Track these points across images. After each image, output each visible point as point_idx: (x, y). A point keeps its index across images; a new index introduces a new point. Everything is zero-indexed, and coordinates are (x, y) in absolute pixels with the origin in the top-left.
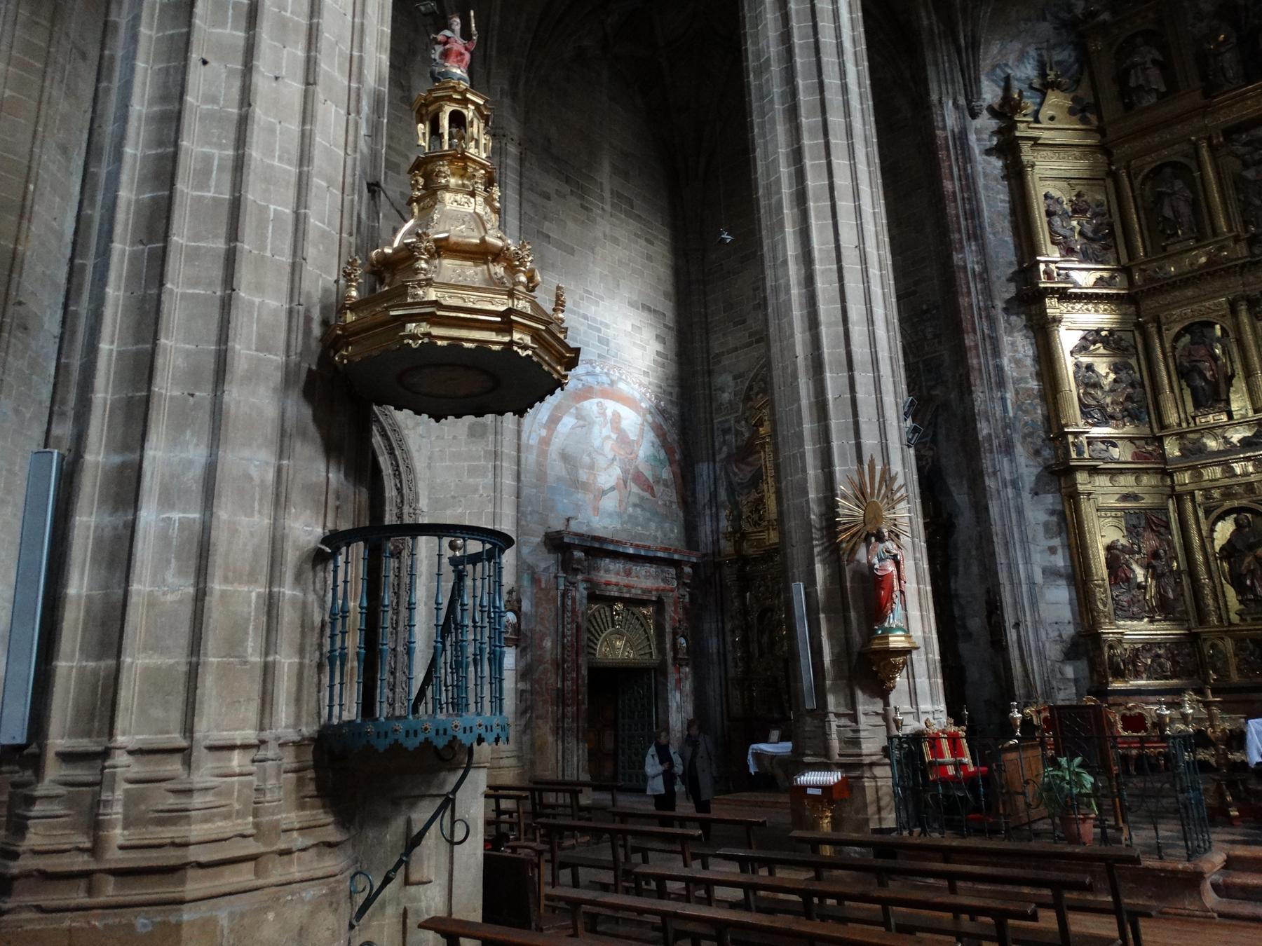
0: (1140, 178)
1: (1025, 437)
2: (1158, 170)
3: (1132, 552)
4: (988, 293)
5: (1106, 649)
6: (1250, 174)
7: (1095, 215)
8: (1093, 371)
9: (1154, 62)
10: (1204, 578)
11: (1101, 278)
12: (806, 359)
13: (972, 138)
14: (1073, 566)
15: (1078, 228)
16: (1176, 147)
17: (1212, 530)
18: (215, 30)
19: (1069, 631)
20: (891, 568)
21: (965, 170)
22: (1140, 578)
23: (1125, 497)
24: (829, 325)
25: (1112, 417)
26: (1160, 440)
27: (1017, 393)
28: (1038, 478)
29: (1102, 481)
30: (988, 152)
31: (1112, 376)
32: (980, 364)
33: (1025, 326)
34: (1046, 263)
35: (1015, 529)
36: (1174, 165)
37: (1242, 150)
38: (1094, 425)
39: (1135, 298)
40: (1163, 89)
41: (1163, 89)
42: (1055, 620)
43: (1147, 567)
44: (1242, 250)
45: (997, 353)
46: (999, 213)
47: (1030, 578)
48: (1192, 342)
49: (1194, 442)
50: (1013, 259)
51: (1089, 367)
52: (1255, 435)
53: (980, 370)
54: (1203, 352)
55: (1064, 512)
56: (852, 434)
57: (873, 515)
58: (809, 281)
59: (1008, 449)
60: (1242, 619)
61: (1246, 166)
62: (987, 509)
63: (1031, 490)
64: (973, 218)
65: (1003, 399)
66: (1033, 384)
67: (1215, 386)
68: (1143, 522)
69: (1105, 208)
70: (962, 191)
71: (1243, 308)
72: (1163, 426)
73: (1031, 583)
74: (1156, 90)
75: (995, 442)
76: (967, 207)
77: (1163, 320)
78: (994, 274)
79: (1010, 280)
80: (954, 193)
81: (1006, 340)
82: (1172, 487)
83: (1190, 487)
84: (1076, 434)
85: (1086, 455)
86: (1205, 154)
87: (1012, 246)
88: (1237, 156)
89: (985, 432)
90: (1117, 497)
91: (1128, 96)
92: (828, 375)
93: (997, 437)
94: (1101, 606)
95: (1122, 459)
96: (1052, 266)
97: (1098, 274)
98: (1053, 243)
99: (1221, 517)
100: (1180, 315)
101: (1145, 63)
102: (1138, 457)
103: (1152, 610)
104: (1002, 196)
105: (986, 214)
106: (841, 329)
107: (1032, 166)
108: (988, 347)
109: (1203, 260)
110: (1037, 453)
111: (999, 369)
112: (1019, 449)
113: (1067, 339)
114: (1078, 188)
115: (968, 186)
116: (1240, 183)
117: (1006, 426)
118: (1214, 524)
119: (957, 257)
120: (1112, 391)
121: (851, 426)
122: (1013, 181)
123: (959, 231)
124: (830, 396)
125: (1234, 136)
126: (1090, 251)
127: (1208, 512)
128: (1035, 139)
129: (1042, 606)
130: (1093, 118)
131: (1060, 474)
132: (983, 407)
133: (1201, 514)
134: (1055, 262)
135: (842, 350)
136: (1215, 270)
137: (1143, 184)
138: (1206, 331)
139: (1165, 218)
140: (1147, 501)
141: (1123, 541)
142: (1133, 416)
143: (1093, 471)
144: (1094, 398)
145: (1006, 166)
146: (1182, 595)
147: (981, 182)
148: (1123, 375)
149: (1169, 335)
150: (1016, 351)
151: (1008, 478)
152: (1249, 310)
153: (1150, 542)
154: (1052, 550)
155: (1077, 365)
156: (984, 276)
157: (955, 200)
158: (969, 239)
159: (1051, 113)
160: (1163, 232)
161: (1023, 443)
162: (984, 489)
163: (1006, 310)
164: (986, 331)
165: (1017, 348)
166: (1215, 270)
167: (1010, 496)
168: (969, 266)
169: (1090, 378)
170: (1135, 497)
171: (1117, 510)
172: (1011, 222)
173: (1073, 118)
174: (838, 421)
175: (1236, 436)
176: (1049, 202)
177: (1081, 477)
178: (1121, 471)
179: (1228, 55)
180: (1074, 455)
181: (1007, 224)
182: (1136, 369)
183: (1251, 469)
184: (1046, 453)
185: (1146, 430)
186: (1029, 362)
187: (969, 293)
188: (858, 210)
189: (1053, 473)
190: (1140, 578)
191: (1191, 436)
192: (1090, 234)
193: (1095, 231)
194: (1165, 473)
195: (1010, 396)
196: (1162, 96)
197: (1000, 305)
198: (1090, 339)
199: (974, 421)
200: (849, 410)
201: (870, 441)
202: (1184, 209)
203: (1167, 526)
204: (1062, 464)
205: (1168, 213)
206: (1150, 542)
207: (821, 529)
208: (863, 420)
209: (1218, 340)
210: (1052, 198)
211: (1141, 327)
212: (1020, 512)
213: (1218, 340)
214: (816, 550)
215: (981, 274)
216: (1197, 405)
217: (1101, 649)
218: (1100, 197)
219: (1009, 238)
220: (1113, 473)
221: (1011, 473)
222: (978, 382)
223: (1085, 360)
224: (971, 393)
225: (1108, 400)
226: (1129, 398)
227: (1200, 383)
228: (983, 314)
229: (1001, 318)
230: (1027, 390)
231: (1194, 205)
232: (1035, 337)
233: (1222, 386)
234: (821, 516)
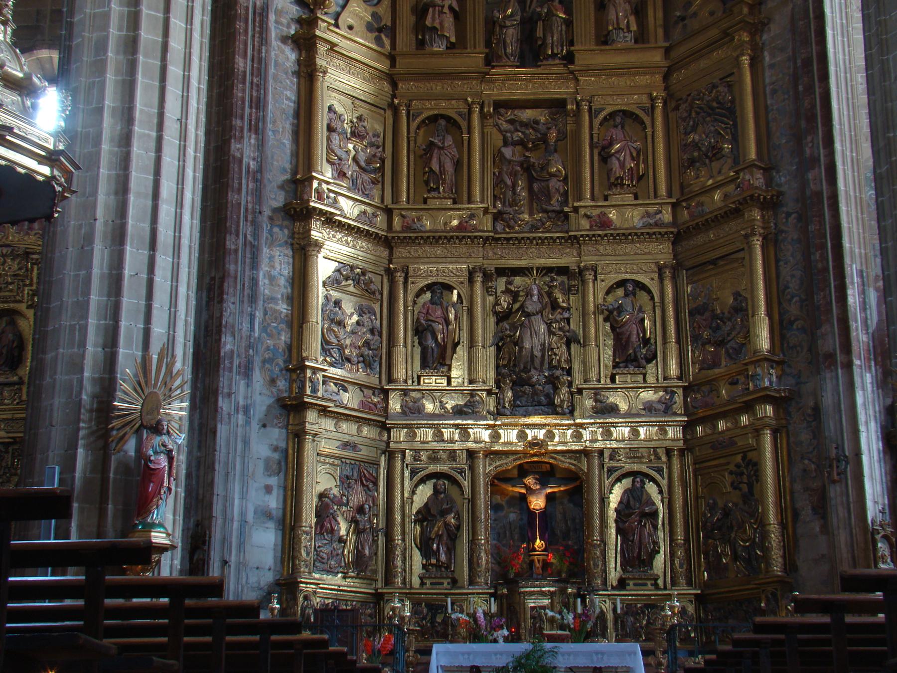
0: (418, 120)
1: (264, 361)
2: (434, 119)
3: (340, 504)
4: (258, 195)
5: (301, 599)
6: (508, 152)
7: (371, 144)
8: (340, 308)
9: (451, 8)
10: (398, 538)
11: (365, 213)
12: (106, 223)
13: (272, 17)
14: (284, 509)
15: (353, 152)
16: (453, 102)
17: (413, 492)
18: (149, 12)
19: (268, 578)
20: (163, 461)
21: (260, 52)
22: (343, 532)
23: (346, 445)
24: (138, 195)
25: (349, 360)
26: (386, 393)
27: (265, 314)
28: (270, 407)
29: (328, 424)
30: (284, 39)
31: (355, 318)
32: (236, 271)
33: (286, 242)
34: (321, 181)
35: (238, 459)
36: (448, 119)
37: (505, 126)
38: (331, 365)
39: (390, 239)
40: (453, 40)
41: (453, 40)
42: (256, 566)
43: (353, 521)
44: (487, 223)
45: (255, 265)
46: (283, 111)
47: (243, 514)
48: (432, 302)
49: (415, 401)
50: (288, 166)
51: (337, 303)
52: (466, 405)
53: (236, 278)
54: (439, 313)
55: (287, 450)
56: (142, 317)
57: (152, 404)
58: (125, 140)
59: (247, 371)
60: (422, 584)
61: (506, 143)
62: (214, 432)
63: (260, 420)
64: (258, 108)
65: (252, 317)
66: (283, 308)
67: (443, 348)
68: (356, 474)
69: (380, 140)
70: (252, 74)
71: (479, 279)
72: (390, 380)
73: (244, 522)
74: (448, 38)
75: (236, 362)
76: (255, 94)
77: (411, 273)
78: (268, 176)
79: (281, 187)
80: (245, 72)
81: (265, 251)
82: (388, 443)
83: (403, 446)
84: (315, 370)
85: (319, 394)
86: (476, 118)
87: (288, 152)
88: (500, 130)
89: (228, 347)
90: (338, 443)
91: (423, 33)
92: (128, 248)
93: (239, 356)
94: (304, 554)
95: (350, 405)
96: (324, 186)
97: (363, 207)
98: (328, 161)
99: (423, 481)
100: (427, 270)
101: (443, 7)
102: (365, 406)
103: (347, 566)
104: (288, 93)
105: (270, 107)
106: (150, 203)
107: (325, 73)
108: (248, 255)
109: (455, 223)
110: (273, 381)
111: (254, 282)
112: (258, 376)
113: (324, 268)
114: (361, 111)
115: (259, 69)
116: (499, 157)
117: (250, 346)
118: (416, 486)
119: (234, 146)
120: (353, 332)
121: (143, 309)
122: (303, 80)
123: (242, 118)
124: (127, 272)
125: (502, 111)
126: (360, 181)
127: (413, 473)
128: (333, 45)
129: (248, 547)
130: (387, 42)
131: (292, 409)
132: (230, 320)
133: (407, 473)
134: (328, 183)
135: (147, 226)
136: (462, 236)
137: (418, 128)
138: (445, 293)
139: (431, 169)
140: (364, 453)
141: (335, 491)
142: (367, 364)
143: (324, 411)
144: (336, 337)
145: (298, 62)
146: (376, 554)
147: (272, 70)
148: (365, 318)
149: (413, 289)
150: (273, 267)
151: (241, 403)
152: (483, 282)
153: (358, 497)
154: (268, 489)
155: (326, 298)
156: (258, 176)
157: (244, 83)
158: (250, 130)
159: (351, 21)
160: (427, 183)
161: (262, 368)
162: (216, 410)
163: (271, 218)
164: (249, 238)
165: (276, 263)
166: (462, 236)
167: (240, 422)
168: (245, 160)
169: (336, 314)
170: (354, 447)
171: (335, 457)
172: (293, 124)
173: (369, 34)
174: (131, 301)
175: (450, 404)
176: (332, 115)
177: (311, 416)
178: (347, 418)
179: (511, 31)
180: (308, 392)
181: (288, 127)
182: (378, 317)
183: (457, 437)
184: (282, 384)
185: (374, 380)
186: (282, 281)
187: (239, 190)
188: (186, 80)
189: (284, 407)
190: (343, 532)
191: (413, 394)
192: (363, 164)
193: (369, 162)
194: (384, 427)
195: (259, 315)
196: (451, 46)
197: (267, 212)
198: (346, 274)
199: (219, 333)
200: (144, 292)
201: (158, 329)
202: (449, 167)
203: (376, 483)
204: (295, 398)
205: (435, 166)
206: (358, 497)
207: (91, 411)
208: (156, 305)
209: (454, 305)
210: (335, 113)
211: (390, 273)
212: (246, 442)
213: (454, 305)
214: (82, 433)
215: (255, 173)
216: (424, 365)
217: (295, 599)
218: (379, 128)
219: (287, 141)
220: (338, 417)
221: (246, 398)
222: (231, 290)
223: (335, 294)
224: (221, 301)
225: (348, 342)
226: (367, 344)
227: (431, 343)
228: (250, 218)
229: (266, 226)
230: (276, 311)
231: (458, 165)
232: (293, 257)
233: (449, 351)
234: (94, 396)
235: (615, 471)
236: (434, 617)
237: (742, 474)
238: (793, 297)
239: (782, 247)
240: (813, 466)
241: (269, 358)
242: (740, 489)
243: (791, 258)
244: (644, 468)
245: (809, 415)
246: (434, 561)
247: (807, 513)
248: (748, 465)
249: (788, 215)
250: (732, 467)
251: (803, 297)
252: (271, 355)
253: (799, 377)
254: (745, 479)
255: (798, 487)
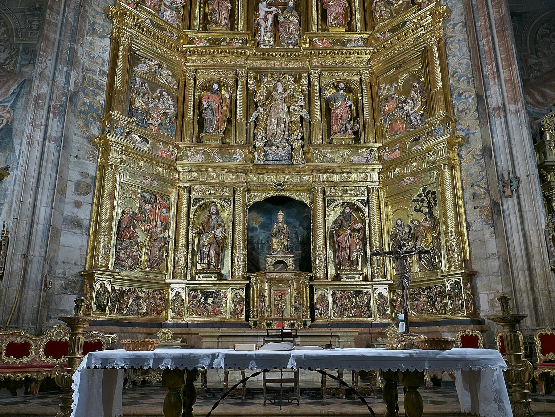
53: (54, 43)
235: (333, 202)
236: (206, 300)
237: (423, 201)
238: (460, 78)
239: (451, 47)
240: (482, 191)
241: (85, 111)
242: (422, 212)
243: (458, 53)
244: (352, 200)
245: (477, 155)
246: (206, 261)
247: (478, 224)
248: (427, 196)
249: (455, 25)
250: (415, 197)
251: (470, 76)
252: (87, 109)
253: (468, 130)
254: (425, 204)
255: (470, 206)
